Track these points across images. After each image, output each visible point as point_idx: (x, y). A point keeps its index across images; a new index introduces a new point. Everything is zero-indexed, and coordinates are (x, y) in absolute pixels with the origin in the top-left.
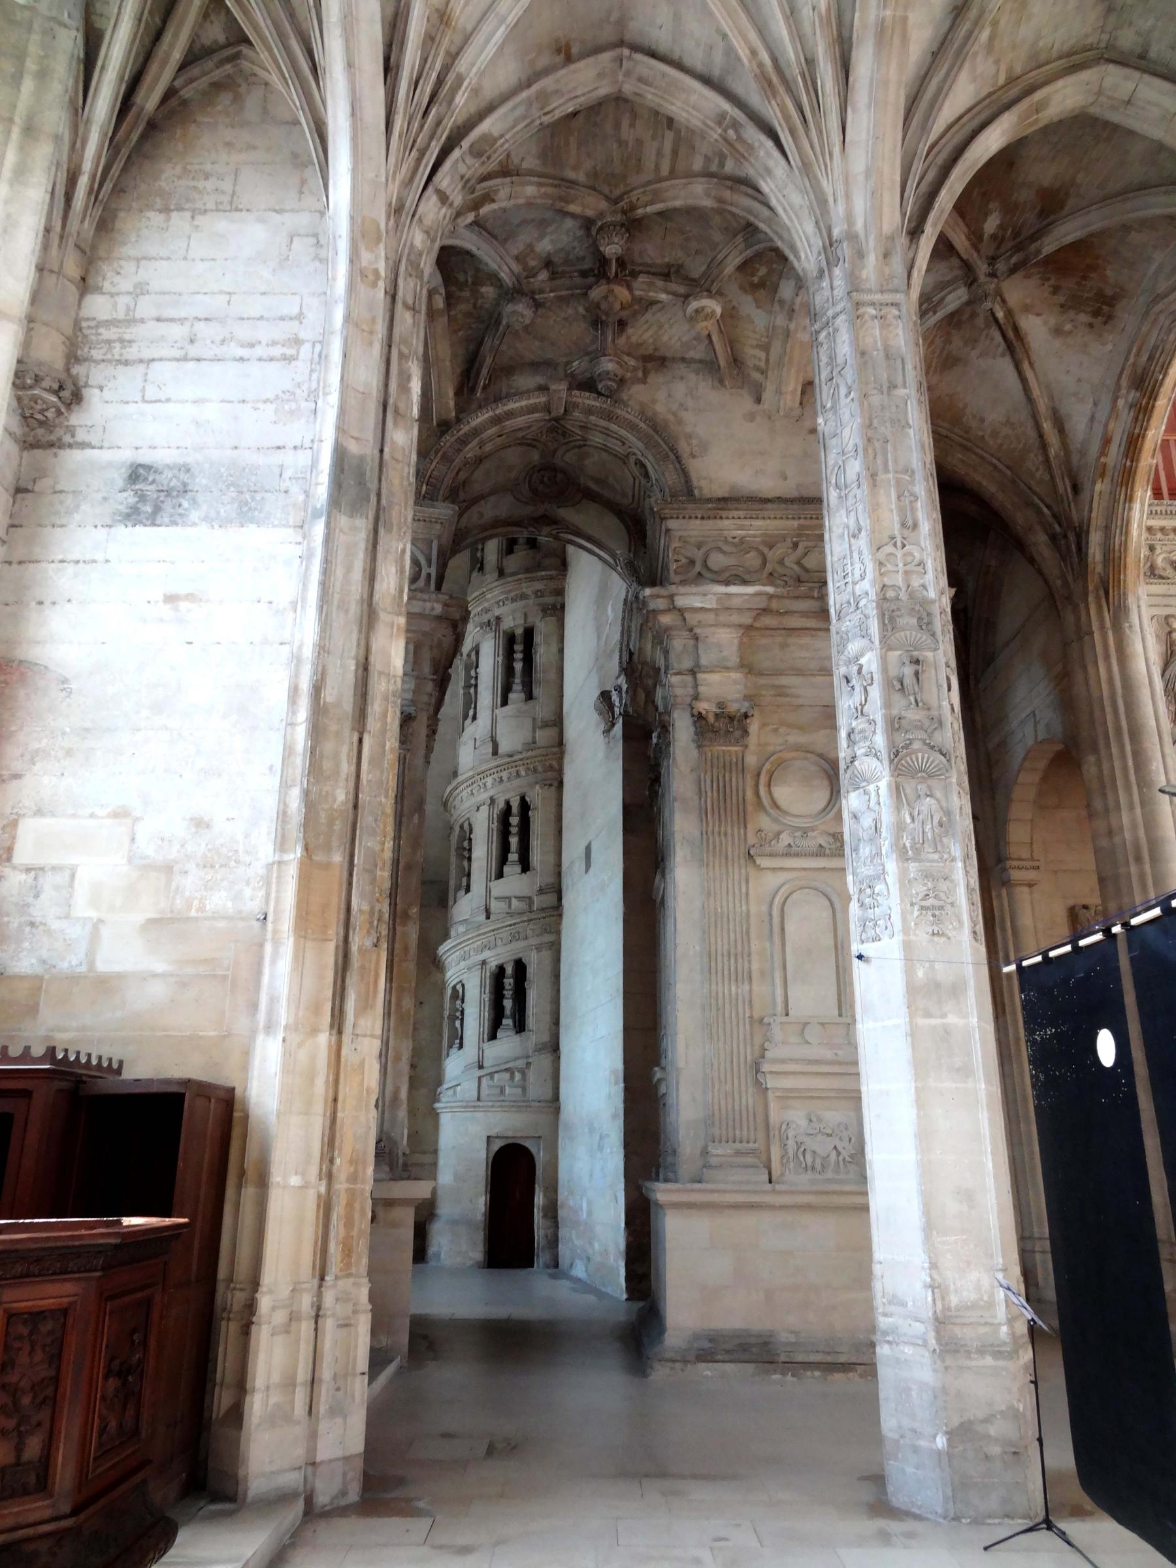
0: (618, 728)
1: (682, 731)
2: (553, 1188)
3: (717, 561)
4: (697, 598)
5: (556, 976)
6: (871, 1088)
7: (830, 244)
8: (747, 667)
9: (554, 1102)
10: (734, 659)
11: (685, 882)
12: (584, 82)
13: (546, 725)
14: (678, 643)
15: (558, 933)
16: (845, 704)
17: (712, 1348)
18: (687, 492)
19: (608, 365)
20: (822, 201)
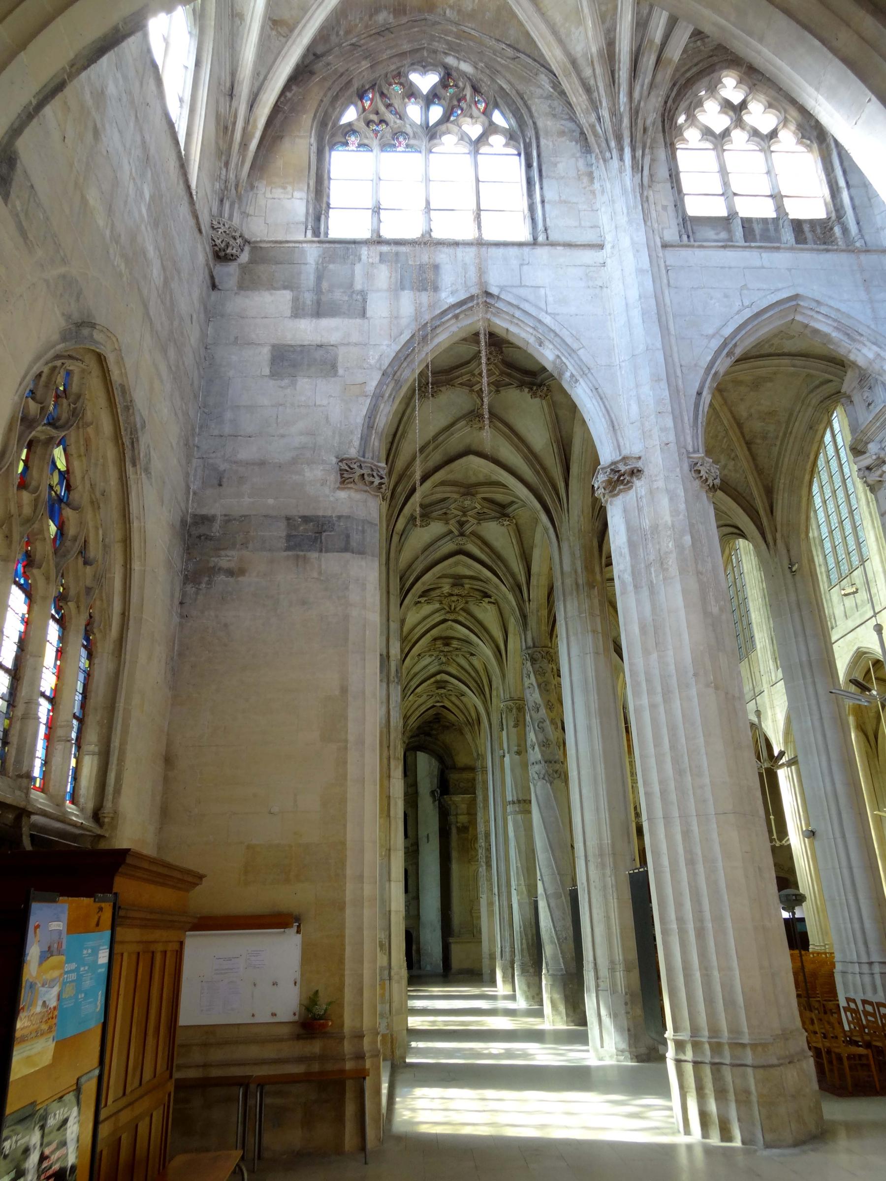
0: (437, 803)
1: (454, 831)
2: (418, 943)
3: (462, 785)
4: (457, 798)
5: (418, 874)
6: (482, 919)
7: (478, 754)
8: (468, 814)
9: (418, 916)
10: (465, 812)
11: (455, 867)
12: (431, 712)
13: (412, 786)
14: (453, 807)
15: (418, 859)
16: (480, 851)
17: (461, 972)
18: (454, 768)
19: (434, 732)
20: (476, 745)
